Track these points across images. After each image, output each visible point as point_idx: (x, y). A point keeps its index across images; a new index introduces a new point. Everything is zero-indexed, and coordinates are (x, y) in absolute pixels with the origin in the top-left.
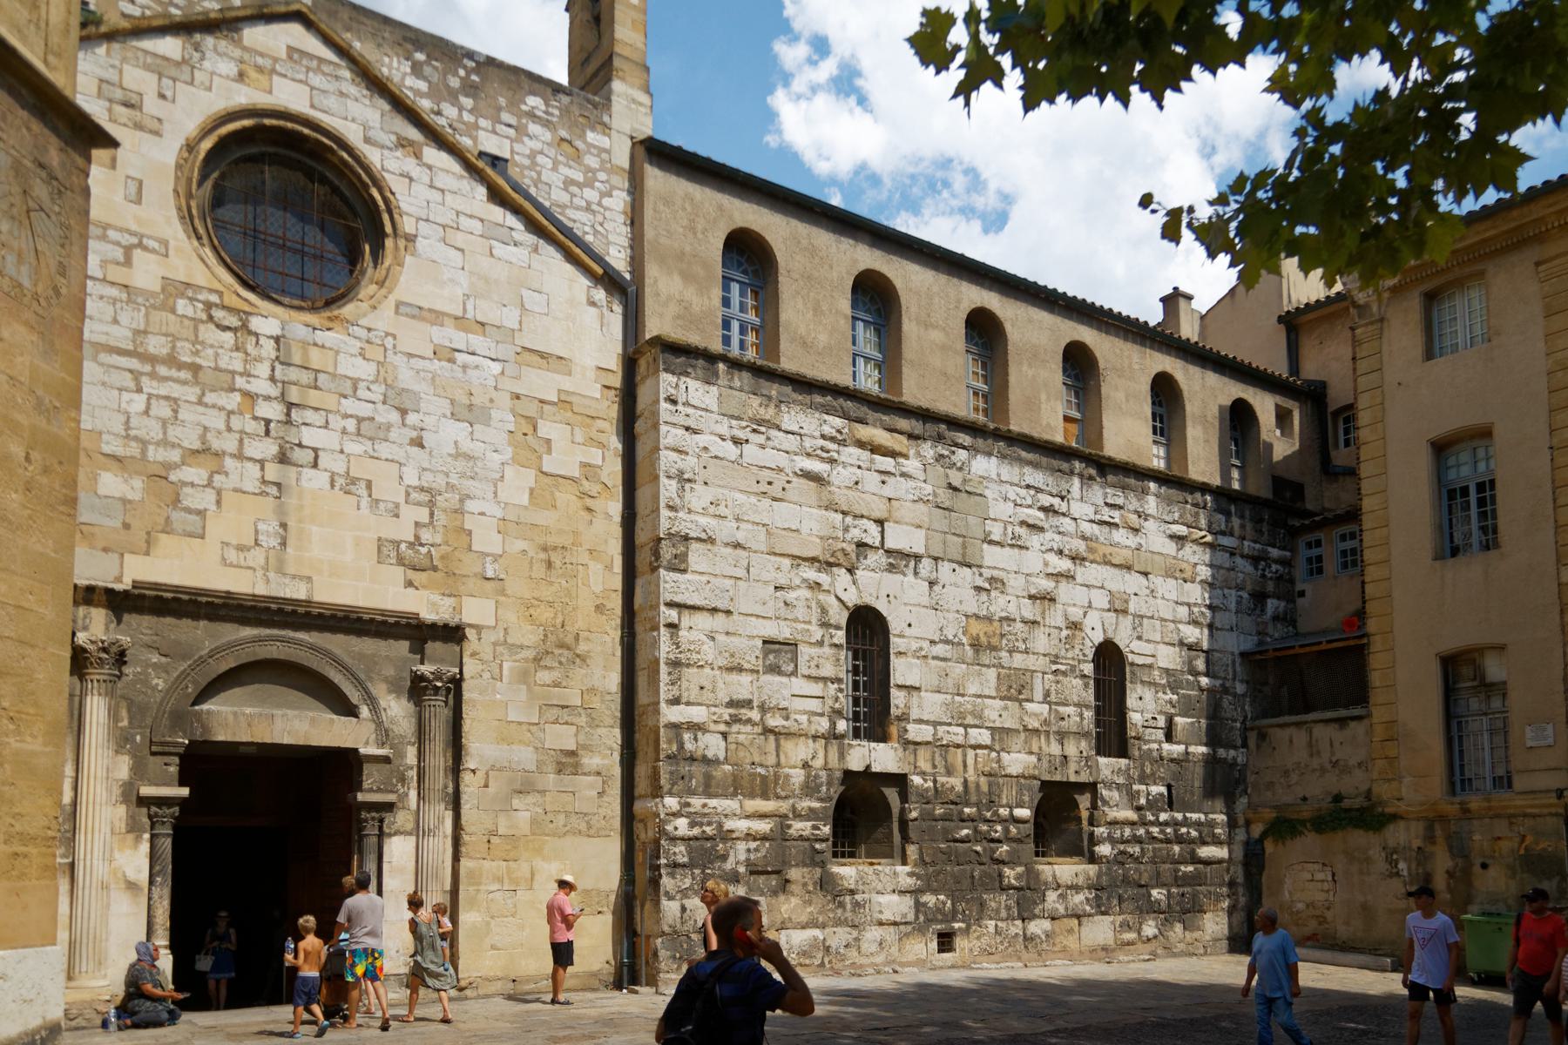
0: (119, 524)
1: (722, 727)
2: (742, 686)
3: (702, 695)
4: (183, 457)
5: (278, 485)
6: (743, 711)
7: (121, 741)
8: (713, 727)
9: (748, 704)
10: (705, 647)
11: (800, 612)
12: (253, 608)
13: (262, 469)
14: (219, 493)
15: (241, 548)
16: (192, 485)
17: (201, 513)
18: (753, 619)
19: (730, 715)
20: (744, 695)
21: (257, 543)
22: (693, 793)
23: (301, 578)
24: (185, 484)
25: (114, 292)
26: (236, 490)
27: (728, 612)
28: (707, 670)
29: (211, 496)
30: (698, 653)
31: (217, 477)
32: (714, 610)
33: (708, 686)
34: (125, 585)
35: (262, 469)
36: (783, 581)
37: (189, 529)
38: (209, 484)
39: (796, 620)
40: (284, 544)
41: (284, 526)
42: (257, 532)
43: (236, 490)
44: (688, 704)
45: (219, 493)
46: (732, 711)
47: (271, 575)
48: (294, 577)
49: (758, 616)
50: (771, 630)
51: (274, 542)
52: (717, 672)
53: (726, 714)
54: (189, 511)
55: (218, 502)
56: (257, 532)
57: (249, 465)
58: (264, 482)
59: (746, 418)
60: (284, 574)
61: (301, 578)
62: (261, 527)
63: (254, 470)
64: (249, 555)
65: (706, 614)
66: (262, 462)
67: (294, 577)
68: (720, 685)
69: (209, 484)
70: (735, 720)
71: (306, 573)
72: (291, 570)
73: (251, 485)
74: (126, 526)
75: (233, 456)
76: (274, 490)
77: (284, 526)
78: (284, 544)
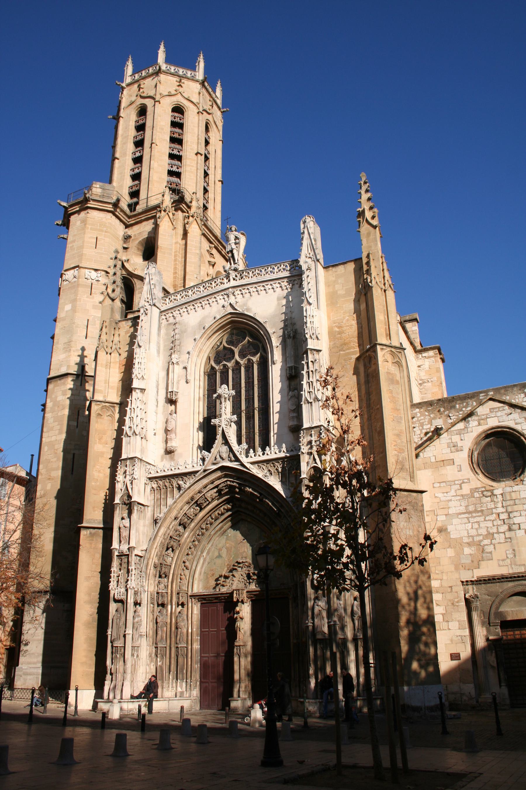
0: (470, 562)
4: (483, 538)
5: (510, 538)
7: (483, 623)
12: (511, 578)
13: (505, 534)
14: (494, 545)
15: (503, 560)
16: (487, 545)
17: (491, 553)
21: (507, 558)
23: (522, 565)
24: (485, 545)
25: (459, 498)
26: (499, 543)
29: (492, 546)
31: (493, 541)
34: (475, 578)
35: (505, 534)
37: (488, 558)
38: (491, 544)
40: (515, 556)
41: (514, 550)
42: (506, 554)
43: (499, 543)
45: (494, 545)
47: (513, 566)
48: (520, 565)
51: (512, 556)
54: (487, 553)
55: (495, 548)
56: (506, 554)
57: (501, 534)
58: (506, 538)
60: (517, 565)
61: (522, 565)
62: (508, 552)
63: (502, 535)
64: (506, 562)
66: (504, 533)
67: (520, 565)
69: (491, 544)
71: (523, 563)
72: (518, 563)
73: (503, 540)
74: (472, 561)
75: (496, 533)
76: (509, 540)
77: (514, 550)
78: (515, 556)
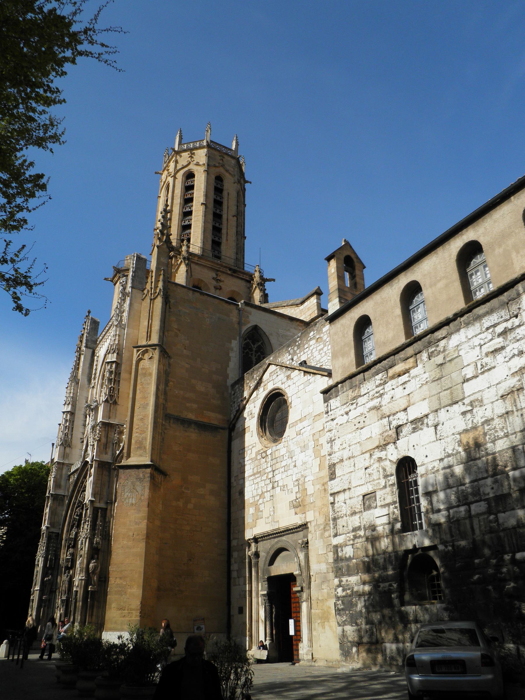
1: (351, 542)
2: (355, 521)
3: (343, 530)
6: (358, 532)
8: (348, 543)
9: (359, 528)
10: (343, 508)
11: (375, 476)
18: (358, 487)
19: (353, 536)
20: (357, 524)
22: (343, 575)
27: (349, 489)
28: (345, 518)
30: (341, 511)
32: (344, 490)
33: (345, 525)
36: (367, 465)
39: (374, 480)
44: (340, 535)
46: (353, 534)
49: (359, 485)
50: (364, 490)
52: (348, 517)
53: (351, 535)
59: (349, 401)
65: (342, 493)
68: (349, 523)
70: (355, 537)
